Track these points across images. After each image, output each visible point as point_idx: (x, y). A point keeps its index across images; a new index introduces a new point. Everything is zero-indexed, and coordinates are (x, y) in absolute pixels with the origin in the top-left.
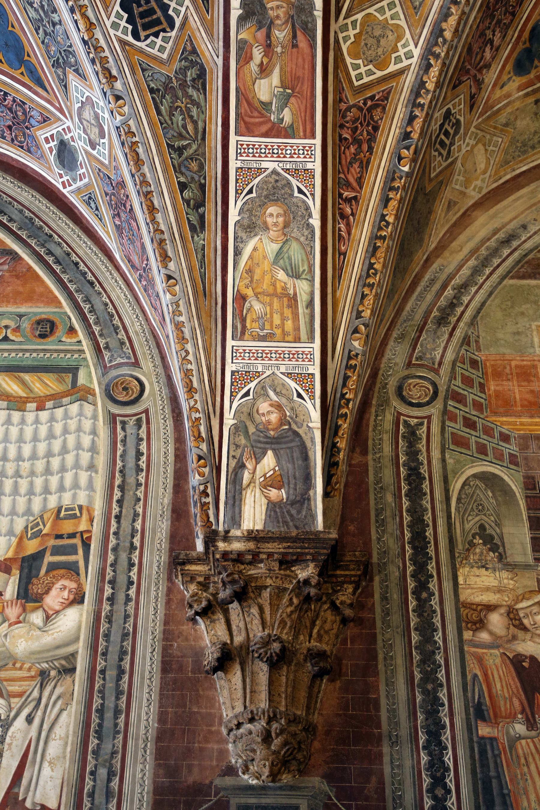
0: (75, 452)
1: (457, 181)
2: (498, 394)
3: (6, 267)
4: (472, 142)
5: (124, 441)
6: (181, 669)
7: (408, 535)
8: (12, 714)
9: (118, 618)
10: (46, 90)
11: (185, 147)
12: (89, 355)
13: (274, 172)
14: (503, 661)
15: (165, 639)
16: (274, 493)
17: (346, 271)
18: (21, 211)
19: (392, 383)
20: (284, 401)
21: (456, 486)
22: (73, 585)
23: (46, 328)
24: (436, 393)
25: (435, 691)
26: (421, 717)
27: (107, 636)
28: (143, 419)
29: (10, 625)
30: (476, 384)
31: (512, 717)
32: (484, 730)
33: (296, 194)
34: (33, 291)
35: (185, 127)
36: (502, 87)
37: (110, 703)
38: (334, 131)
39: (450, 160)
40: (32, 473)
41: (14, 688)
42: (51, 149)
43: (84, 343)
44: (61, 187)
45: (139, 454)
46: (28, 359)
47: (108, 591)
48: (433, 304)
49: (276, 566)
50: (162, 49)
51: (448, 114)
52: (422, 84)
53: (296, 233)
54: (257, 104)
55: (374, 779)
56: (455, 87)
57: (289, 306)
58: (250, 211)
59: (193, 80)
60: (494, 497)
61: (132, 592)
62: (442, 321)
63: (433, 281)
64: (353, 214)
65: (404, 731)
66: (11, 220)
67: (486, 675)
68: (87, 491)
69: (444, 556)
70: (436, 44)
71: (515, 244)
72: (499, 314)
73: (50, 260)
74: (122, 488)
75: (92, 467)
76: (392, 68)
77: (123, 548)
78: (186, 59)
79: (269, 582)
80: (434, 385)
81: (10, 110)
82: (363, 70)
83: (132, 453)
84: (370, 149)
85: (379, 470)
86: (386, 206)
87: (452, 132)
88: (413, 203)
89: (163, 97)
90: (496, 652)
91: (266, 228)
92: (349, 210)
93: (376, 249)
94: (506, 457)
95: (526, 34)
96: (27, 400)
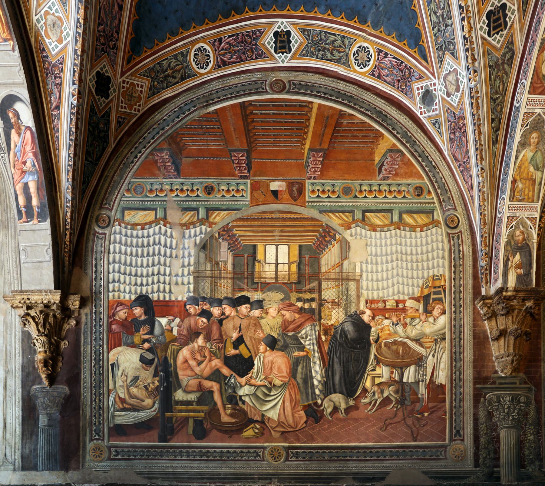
3: (399, 159)
5: (454, 245)
6: (479, 338)
9: (458, 319)
10: (427, 62)
12: (437, 204)
15: (474, 327)
18: (401, 128)
22: (442, 307)
23: (419, 191)
27: (455, 326)
28: (459, 236)
34: (412, 172)
37: (458, 350)
40: (423, 261)
41: (427, 345)
42: (419, 94)
44: (419, 114)
45: (460, 251)
46: (414, 206)
47: (453, 309)
61: (462, 309)
66: (398, 133)
68: (442, 268)
73: (417, 155)
74: (455, 266)
77: (457, 292)
81: (402, 71)
83: (457, 251)
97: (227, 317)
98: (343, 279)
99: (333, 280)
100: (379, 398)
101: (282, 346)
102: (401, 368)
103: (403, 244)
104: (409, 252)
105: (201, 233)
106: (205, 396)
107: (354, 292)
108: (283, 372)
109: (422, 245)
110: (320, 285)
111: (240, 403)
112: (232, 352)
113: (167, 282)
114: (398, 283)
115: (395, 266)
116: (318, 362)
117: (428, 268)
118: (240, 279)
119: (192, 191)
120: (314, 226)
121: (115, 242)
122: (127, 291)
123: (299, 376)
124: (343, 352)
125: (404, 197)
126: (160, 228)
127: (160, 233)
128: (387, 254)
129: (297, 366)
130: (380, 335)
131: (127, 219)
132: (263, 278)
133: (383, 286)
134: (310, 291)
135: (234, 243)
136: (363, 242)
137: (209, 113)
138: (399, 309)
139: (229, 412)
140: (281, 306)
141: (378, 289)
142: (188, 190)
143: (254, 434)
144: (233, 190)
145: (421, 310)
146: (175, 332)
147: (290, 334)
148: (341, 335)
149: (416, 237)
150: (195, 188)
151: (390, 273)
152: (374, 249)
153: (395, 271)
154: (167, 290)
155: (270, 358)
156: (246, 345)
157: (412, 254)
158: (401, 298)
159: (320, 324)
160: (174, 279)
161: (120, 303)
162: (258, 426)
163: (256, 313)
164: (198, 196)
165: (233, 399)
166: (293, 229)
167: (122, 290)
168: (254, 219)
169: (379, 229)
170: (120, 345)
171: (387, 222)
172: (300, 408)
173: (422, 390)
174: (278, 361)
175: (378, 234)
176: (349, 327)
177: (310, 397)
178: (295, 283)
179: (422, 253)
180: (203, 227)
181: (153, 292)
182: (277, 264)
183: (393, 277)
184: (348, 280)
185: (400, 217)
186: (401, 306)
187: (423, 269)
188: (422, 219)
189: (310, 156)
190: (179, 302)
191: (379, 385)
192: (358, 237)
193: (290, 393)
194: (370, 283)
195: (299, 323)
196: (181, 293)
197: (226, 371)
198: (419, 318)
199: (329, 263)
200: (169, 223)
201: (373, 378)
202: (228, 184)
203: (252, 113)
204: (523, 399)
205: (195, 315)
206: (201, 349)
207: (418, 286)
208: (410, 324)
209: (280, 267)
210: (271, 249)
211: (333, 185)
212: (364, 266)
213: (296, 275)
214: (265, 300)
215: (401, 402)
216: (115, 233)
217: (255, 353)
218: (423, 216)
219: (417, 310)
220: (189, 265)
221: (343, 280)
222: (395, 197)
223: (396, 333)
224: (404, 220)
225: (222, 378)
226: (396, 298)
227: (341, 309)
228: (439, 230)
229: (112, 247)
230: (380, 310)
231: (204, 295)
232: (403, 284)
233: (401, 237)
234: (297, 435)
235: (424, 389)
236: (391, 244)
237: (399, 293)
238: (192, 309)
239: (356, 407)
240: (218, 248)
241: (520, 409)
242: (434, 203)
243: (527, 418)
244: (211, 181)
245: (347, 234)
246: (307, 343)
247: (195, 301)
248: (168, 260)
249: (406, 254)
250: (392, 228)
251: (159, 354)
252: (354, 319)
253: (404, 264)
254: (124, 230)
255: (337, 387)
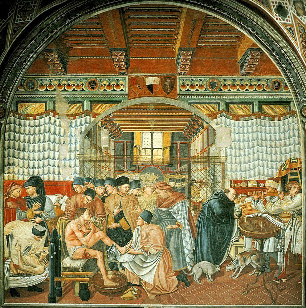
0: (293, 138)
8: (286, 228)
22: (298, 187)
23: (277, 85)
29: (281, 200)
41: (285, 220)
43: (291, 92)
75: (299, 143)
96: (275, 116)
97: (109, 195)
98: (210, 162)
99: (201, 163)
100: (242, 265)
101: (157, 220)
102: (262, 240)
103: (263, 131)
104: (268, 139)
105: (86, 122)
106: (90, 264)
107: (219, 173)
108: (158, 243)
109: (280, 132)
110: (190, 167)
111: (120, 269)
112: (114, 225)
113: (56, 165)
114: (259, 165)
115: (255, 151)
116: (188, 234)
117: (286, 153)
118: (120, 162)
119: (78, 86)
120: (185, 116)
121: (10, 130)
122: (21, 172)
123: (172, 246)
124: (210, 226)
125: (264, 90)
126: (50, 118)
127: (50, 122)
128: (248, 141)
129: (170, 237)
130: (243, 210)
131: (20, 110)
132: (140, 161)
133: (245, 168)
134: (182, 172)
135: (115, 131)
136: (228, 129)
137: (92, 18)
138: (259, 188)
139: (110, 277)
140: (156, 186)
141: (241, 171)
142: (74, 85)
143: (132, 296)
144: (113, 85)
145: (279, 189)
146: (63, 208)
147: (164, 210)
148: (208, 210)
149: (275, 125)
150: (80, 83)
151: (251, 157)
152: (237, 136)
153: (256, 155)
154: (56, 172)
155: (147, 231)
156: (126, 219)
157: (271, 140)
158: (262, 179)
159: (190, 201)
160: (63, 162)
161: (15, 183)
162: (136, 290)
163: (135, 191)
164: (83, 90)
165: (114, 266)
166: (166, 119)
167: (17, 172)
168: (132, 111)
169: (241, 118)
170: (14, 219)
171: (249, 113)
172: (172, 273)
173: (281, 259)
174: (153, 233)
175: (241, 123)
176: (215, 204)
177: (181, 264)
178: (169, 166)
179: (280, 140)
180: (88, 117)
181: (44, 174)
182: (152, 149)
183: (254, 160)
184: (215, 162)
185: (261, 108)
186: (261, 185)
187: (281, 153)
188: (280, 110)
189: (181, 55)
190: (67, 182)
191: (242, 254)
192: (223, 125)
193: (164, 260)
194: (234, 166)
195: (172, 200)
196: (68, 175)
197: (108, 241)
198: (278, 196)
199: (198, 148)
200: (58, 114)
201: (237, 248)
202: (109, 80)
203: (129, 17)
205: (81, 193)
206: (86, 223)
207: (277, 168)
208: (270, 202)
209: (155, 151)
210: (147, 136)
211: (201, 80)
212: (228, 150)
213: (169, 159)
214: (142, 181)
215: (262, 269)
216: (10, 123)
217: (133, 225)
218: (281, 107)
219: (276, 189)
220: (75, 150)
221: (210, 163)
222: (255, 90)
223: (257, 209)
224: (264, 110)
225: (105, 247)
226: (257, 178)
227: (208, 188)
228: (295, 119)
229: (7, 134)
230: (242, 189)
231: (89, 176)
232: (263, 166)
233: (261, 125)
234: (170, 297)
235: (282, 258)
236: (253, 132)
237: (259, 174)
238: (78, 188)
239: (221, 273)
240: (101, 134)
242: (291, 95)
244: (94, 77)
245: (213, 123)
246: (179, 217)
247: (81, 181)
248: (57, 146)
249: (266, 140)
250: (253, 117)
251: (49, 226)
252: (219, 197)
253: (264, 149)
254: (18, 120)
255: (205, 255)
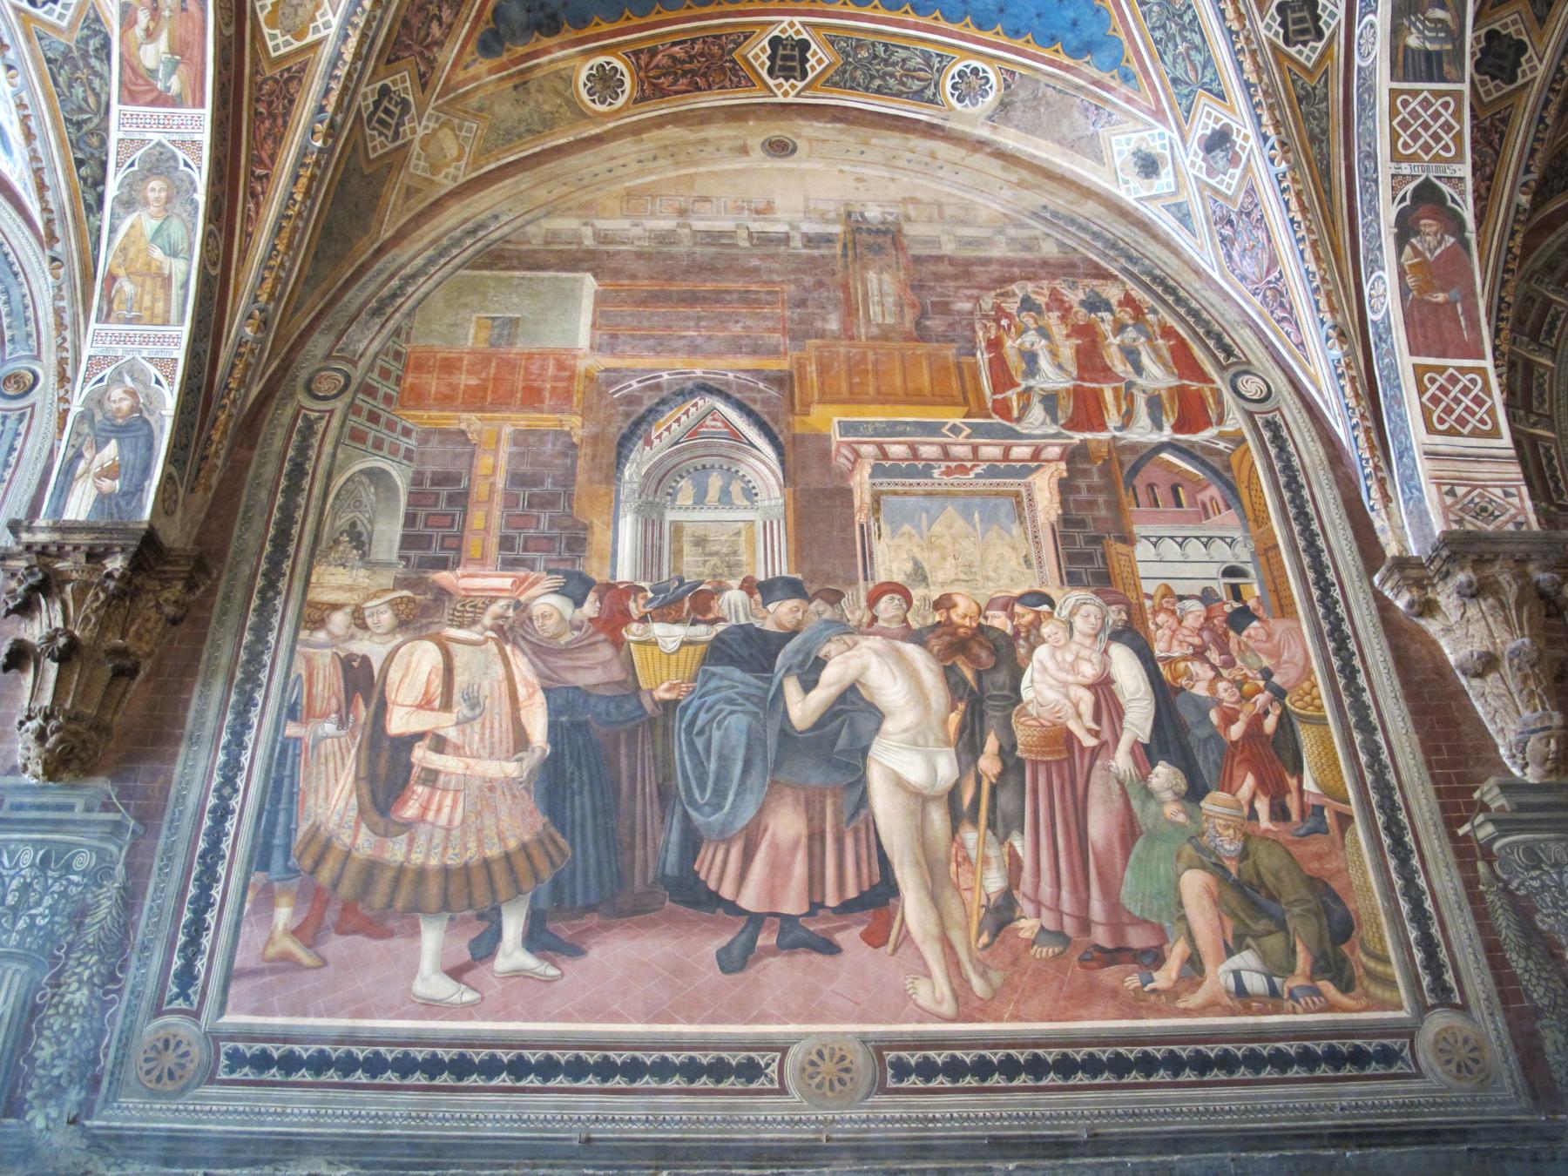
1: (417, 166)
2: (413, 388)
4: (432, 125)
7: (272, 532)
11: (86, 121)
13: (159, 144)
14: (333, 661)
16: (107, 485)
17: (251, 251)
19: (304, 375)
20: (139, 388)
21: (339, 481)
24: (346, 386)
25: (253, 691)
26: (229, 717)
30: (393, 377)
31: (325, 716)
32: (292, 730)
33: (182, 167)
35: (85, 100)
36: (466, 68)
38: (250, 104)
39: (400, 142)
48: (373, 295)
49: (83, 559)
50: (61, 17)
51: (385, 92)
52: (340, 55)
53: (178, 209)
54: (142, 71)
55: (161, 778)
56: (389, 62)
57: (163, 287)
58: (130, 185)
59: (96, 50)
60: (376, 493)
62: (377, 312)
63: (380, 272)
64: (263, 193)
65: (208, 731)
67: (310, 675)
69: (303, 554)
70: (355, 13)
71: (481, 234)
72: (441, 305)
76: (310, 38)
78: (88, 27)
79: (75, 575)
80: (348, 378)
82: (280, 40)
84: (285, 123)
85: (262, 465)
86: (295, 184)
87: (397, 111)
88: (341, 183)
89: (61, 67)
90: (328, 652)
91: (146, 203)
92: (259, 189)
93: (281, 228)
94: (402, 451)
95: (488, 14)
204: (84, 860)
241: (63, 894)
243: (80, 925)
